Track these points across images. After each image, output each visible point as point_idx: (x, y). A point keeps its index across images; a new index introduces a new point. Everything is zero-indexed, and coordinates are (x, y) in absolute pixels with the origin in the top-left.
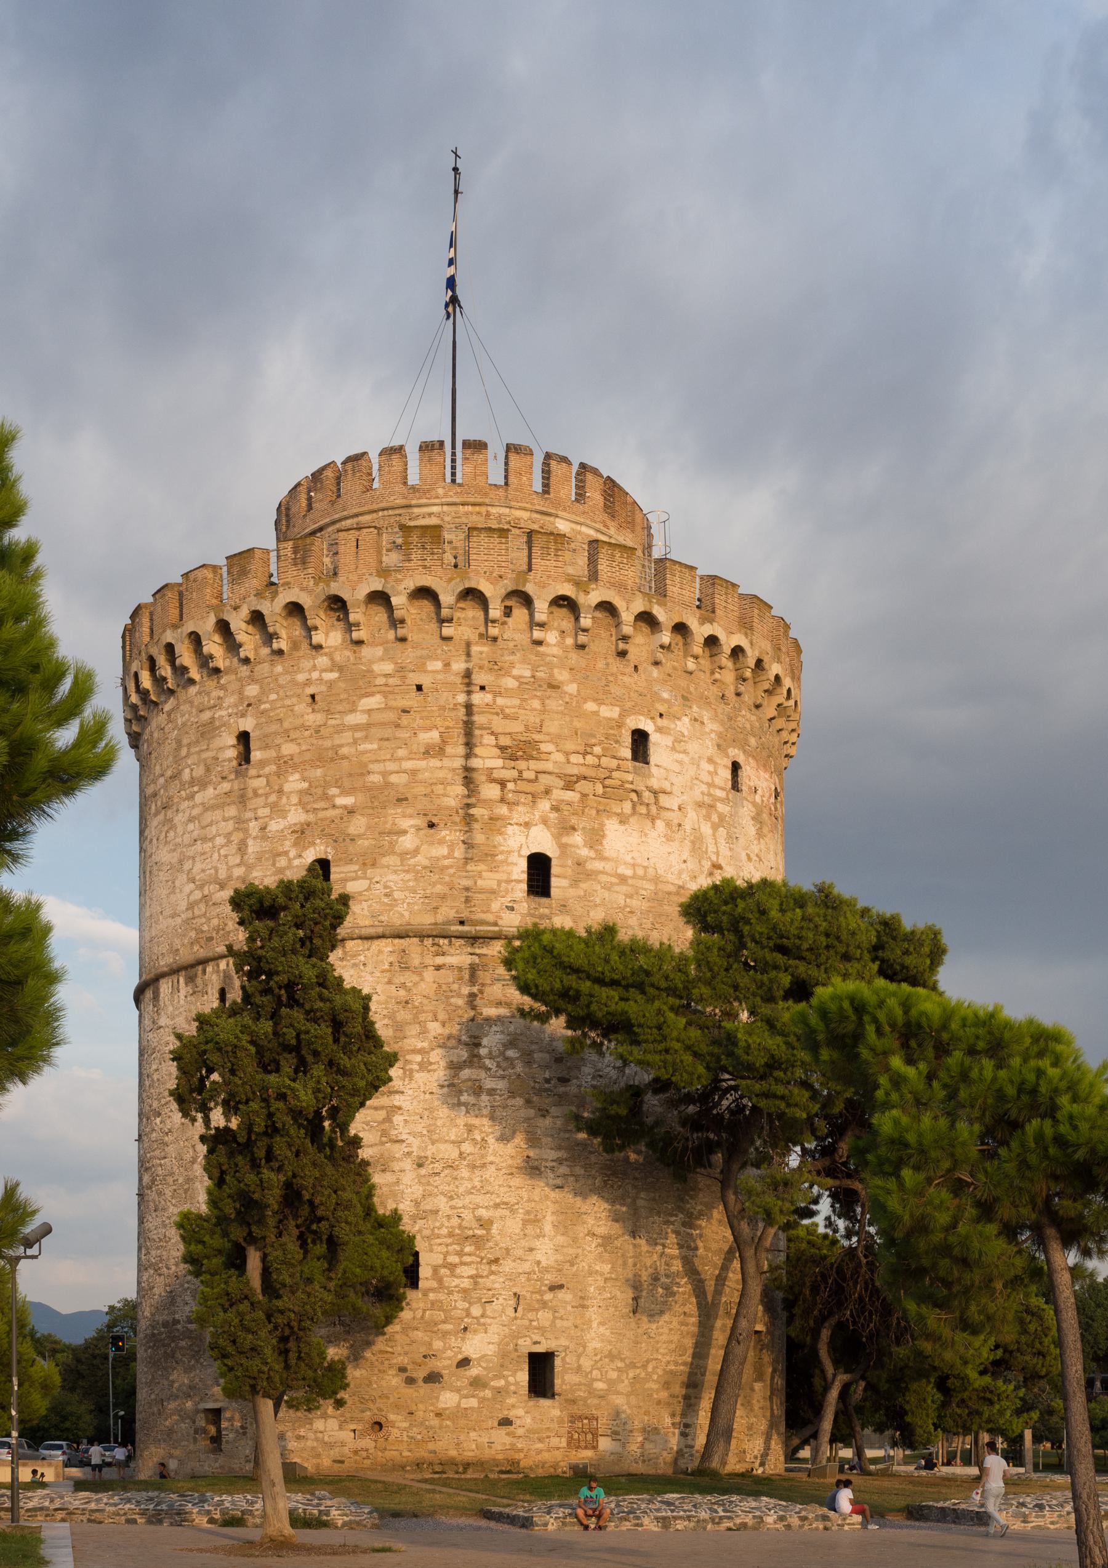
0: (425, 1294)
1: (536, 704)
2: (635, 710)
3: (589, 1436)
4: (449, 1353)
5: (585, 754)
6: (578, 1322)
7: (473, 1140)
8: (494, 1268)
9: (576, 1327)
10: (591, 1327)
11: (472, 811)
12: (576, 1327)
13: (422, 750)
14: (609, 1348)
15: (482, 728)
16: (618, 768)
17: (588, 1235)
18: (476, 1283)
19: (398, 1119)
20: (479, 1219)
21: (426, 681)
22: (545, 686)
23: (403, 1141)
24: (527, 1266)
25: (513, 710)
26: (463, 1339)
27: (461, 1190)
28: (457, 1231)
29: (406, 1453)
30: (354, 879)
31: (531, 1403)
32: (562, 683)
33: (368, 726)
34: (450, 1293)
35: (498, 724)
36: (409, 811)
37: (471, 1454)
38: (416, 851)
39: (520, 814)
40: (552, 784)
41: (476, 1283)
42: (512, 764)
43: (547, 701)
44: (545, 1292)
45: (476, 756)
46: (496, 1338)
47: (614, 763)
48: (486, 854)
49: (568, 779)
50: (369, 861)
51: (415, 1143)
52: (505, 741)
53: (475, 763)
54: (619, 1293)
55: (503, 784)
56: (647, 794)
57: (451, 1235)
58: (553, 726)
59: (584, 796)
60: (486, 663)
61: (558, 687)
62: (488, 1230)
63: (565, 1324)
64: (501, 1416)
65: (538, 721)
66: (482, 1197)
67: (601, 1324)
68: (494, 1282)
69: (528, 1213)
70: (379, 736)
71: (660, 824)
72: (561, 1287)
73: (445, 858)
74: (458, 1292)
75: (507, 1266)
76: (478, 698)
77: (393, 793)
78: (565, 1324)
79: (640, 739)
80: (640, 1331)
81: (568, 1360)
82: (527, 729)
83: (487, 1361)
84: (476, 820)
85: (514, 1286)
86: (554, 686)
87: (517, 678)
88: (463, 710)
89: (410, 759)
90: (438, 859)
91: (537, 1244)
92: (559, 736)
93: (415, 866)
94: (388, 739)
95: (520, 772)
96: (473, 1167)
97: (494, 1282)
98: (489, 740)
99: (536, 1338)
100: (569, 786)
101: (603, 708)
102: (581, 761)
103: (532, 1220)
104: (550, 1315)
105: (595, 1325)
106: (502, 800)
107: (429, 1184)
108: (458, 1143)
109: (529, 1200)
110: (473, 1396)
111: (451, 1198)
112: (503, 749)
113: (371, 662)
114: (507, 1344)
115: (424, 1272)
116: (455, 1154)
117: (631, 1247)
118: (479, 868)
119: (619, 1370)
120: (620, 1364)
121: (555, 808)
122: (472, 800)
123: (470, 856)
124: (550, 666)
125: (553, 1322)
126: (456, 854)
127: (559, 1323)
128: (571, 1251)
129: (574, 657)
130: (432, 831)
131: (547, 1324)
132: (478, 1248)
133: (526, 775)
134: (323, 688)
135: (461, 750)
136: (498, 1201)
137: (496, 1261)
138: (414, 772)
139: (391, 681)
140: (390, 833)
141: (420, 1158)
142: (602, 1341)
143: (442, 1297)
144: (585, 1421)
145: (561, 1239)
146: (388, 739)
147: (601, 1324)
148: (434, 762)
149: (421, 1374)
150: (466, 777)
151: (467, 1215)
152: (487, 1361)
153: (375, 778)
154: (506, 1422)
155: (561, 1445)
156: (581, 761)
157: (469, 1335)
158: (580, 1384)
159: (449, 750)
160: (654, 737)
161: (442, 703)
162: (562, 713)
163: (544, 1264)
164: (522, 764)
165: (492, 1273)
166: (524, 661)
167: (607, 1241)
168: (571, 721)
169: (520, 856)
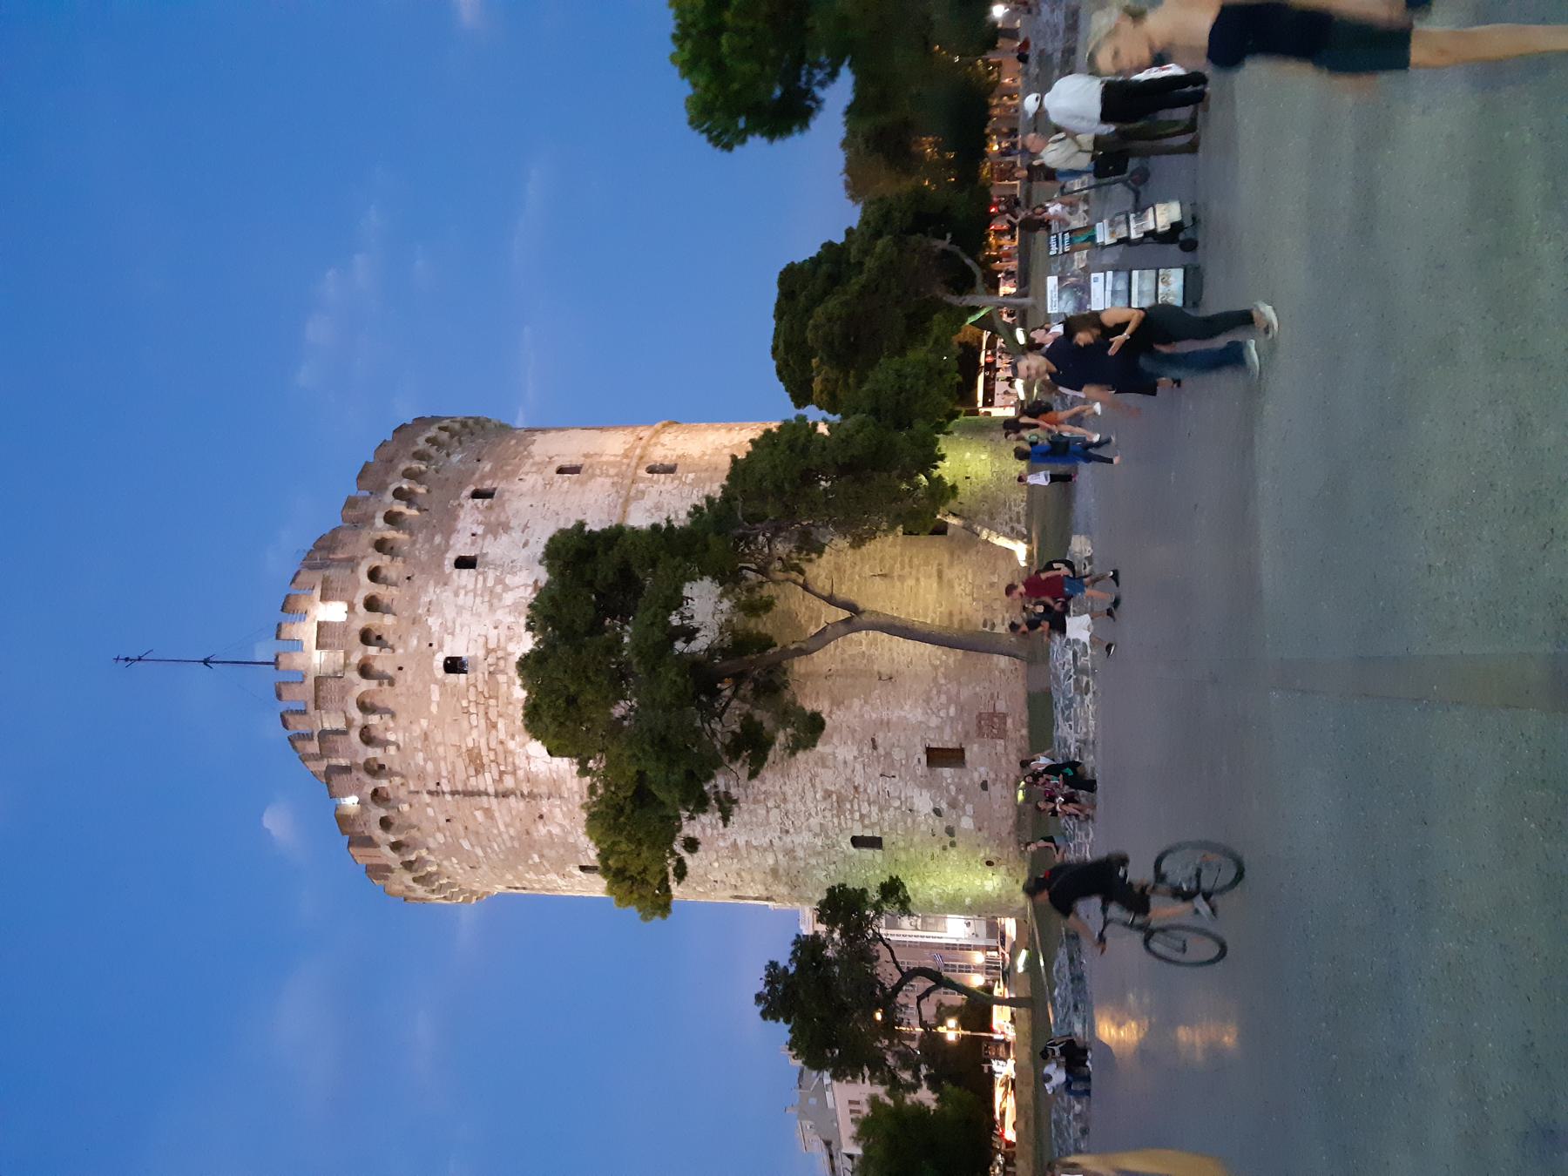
0: (885, 833)
2: (431, 671)
3: (996, 720)
4: (930, 821)
5: (468, 713)
7: (765, 799)
8: (861, 789)
9: (905, 729)
11: (526, 793)
12: (905, 729)
13: (490, 821)
14: (921, 701)
15: (466, 785)
18: (874, 802)
19: (755, 843)
20: (825, 799)
22: (427, 742)
23: (771, 841)
24: (859, 767)
25: (448, 764)
26: (918, 812)
28: (835, 812)
29: (1011, 849)
30: (589, 856)
31: (968, 766)
32: (422, 730)
37: (1011, 810)
38: (561, 825)
39: (521, 762)
41: (874, 802)
45: (486, 789)
46: (917, 791)
47: (472, 689)
53: (491, 790)
54: (877, 692)
56: (491, 660)
57: (839, 817)
58: (453, 738)
59: (500, 715)
61: (425, 734)
62: (832, 792)
63: (902, 738)
64: (980, 789)
67: (902, 708)
68: (873, 790)
69: (816, 764)
72: (873, 740)
74: (882, 813)
75: (858, 780)
76: (446, 787)
77: (524, 837)
79: (454, 665)
81: (932, 737)
82: (458, 756)
83: (935, 796)
84: (532, 790)
86: (426, 736)
88: (457, 796)
89: (498, 827)
91: (840, 758)
95: (492, 761)
96: (785, 800)
98: (473, 781)
99: (916, 761)
100: (494, 726)
103: (822, 762)
105: (903, 714)
106: (514, 773)
107: (800, 827)
109: (807, 763)
110: (964, 807)
111: (810, 814)
112: (477, 772)
113: (439, 843)
114: (921, 782)
115: (868, 833)
116: (775, 812)
119: (939, 692)
120: (934, 692)
121: (513, 737)
122: (518, 793)
127: (903, 742)
128: (845, 731)
129: (403, 720)
133: (492, 758)
134: (464, 864)
135: (485, 798)
137: (856, 788)
138: (507, 826)
139: (448, 834)
141: (781, 832)
142: (916, 707)
144: (983, 722)
145: (835, 740)
147: (902, 708)
148: (497, 814)
149: (948, 839)
150: (503, 796)
151: (821, 806)
152: (935, 796)
153: (516, 844)
154: (984, 786)
155: (1003, 744)
156: (475, 716)
157: (915, 808)
158: (951, 727)
159: (486, 806)
160: (448, 652)
163: (856, 753)
164: (485, 760)
165: (865, 790)
166: (413, 758)
169: (551, 763)
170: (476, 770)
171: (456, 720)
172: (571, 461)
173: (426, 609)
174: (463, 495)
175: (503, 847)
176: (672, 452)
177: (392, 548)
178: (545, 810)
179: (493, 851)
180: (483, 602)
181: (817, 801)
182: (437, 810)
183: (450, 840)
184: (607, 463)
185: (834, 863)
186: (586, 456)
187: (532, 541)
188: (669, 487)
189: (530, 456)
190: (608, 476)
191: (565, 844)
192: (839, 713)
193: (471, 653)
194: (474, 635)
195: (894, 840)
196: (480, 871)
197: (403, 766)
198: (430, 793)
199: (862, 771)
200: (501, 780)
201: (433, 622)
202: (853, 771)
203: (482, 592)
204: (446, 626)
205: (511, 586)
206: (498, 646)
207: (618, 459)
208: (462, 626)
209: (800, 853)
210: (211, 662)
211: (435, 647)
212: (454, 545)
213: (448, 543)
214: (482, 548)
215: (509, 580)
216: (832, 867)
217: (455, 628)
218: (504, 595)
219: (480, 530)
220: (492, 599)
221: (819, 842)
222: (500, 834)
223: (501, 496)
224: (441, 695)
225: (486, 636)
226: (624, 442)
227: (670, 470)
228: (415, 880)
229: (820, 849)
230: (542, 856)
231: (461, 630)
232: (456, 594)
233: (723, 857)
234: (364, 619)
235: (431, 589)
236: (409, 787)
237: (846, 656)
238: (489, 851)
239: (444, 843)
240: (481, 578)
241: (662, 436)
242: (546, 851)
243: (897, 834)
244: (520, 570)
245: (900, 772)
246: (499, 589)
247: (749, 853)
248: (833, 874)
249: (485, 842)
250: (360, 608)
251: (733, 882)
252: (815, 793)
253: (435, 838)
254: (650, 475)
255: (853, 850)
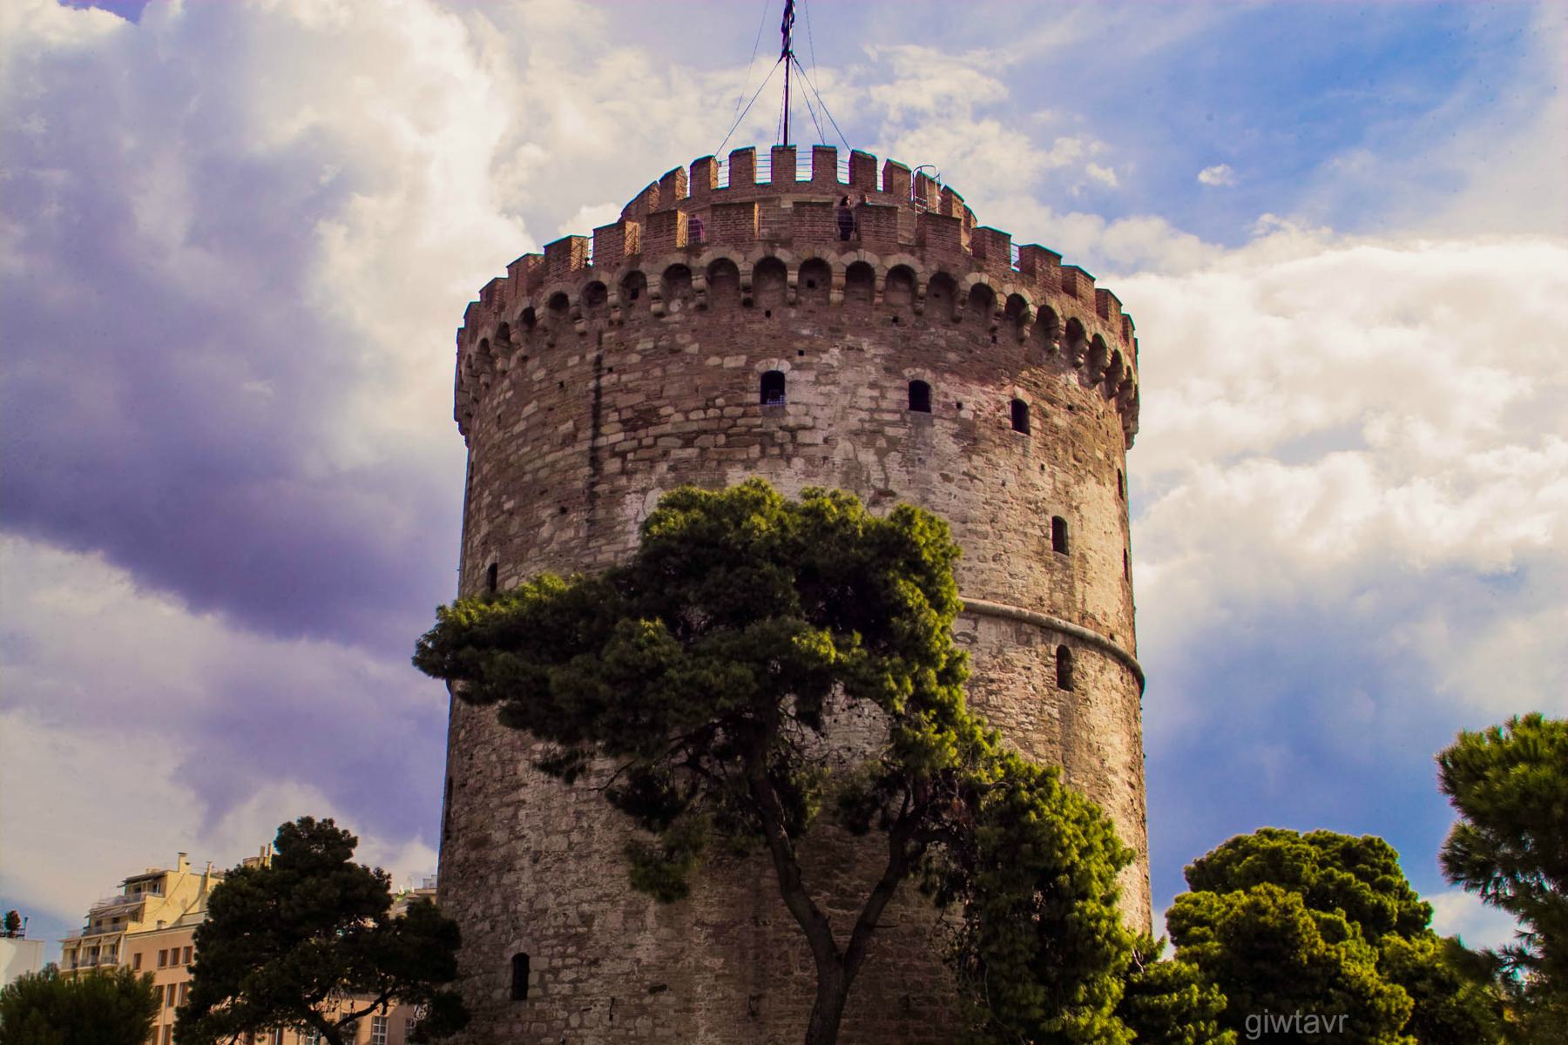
0: (532, 1005)
1: (657, 372)
5: (705, 409)
6: (682, 1029)
7: (582, 827)
8: (593, 970)
10: (697, 1035)
11: (598, 489)
12: (679, 1035)
13: (560, 441)
15: (609, 407)
16: (744, 415)
17: (695, 925)
18: (576, 988)
19: (522, 813)
20: (582, 915)
21: (564, 376)
23: (524, 837)
24: (626, 966)
27: (568, 884)
28: (562, 931)
32: (684, 346)
33: (527, 430)
34: (552, 1002)
35: (623, 400)
36: (547, 502)
39: (639, 481)
40: (669, 444)
41: (576, 988)
42: (633, 434)
43: (668, 367)
44: (645, 995)
45: (602, 435)
47: (740, 410)
48: (606, 528)
49: (687, 436)
50: (519, 558)
51: (532, 836)
52: (627, 414)
53: (602, 441)
54: (733, 993)
55: (623, 455)
57: (556, 935)
58: (671, 390)
59: (703, 450)
60: (614, 346)
63: (666, 1032)
65: (658, 387)
66: (586, 890)
67: (710, 1030)
69: (630, 904)
70: (533, 438)
71: (798, 463)
73: (572, 539)
74: (559, 1000)
75: (607, 967)
76: (606, 381)
78: (666, 1032)
79: (773, 385)
80: (763, 1038)
82: (648, 397)
84: (599, 497)
85: (612, 989)
86: (675, 351)
87: (639, 353)
88: (593, 395)
89: (551, 452)
90: (566, 542)
92: (679, 397)
93: (549, 553)
94: (537, 439)
96: (579, 857)
97: (593, 986)
98: (614, 416)
100: (688, 441)
101: (727, 360)
102: (702, 415)
103: (634, 913)
104: (649, 1023)
105: (702, 1032)
106: (624, 472)
107: (541, 880)
108: (567, 833)
111: (559, 894)
112: (623, 422)
113: (532, 373)
115: (533, 979)
116: (565, 846)
117: (752, 936)
118: (599, 543)
121: (672, 469)
123: (591, 533)
124: (673, 333)
125: (653, 1030)
126: (581, 534)
127: (659, 1031)
128: (676, 945)
129: (696, 320)
130: (564, 516)
131: (645, 1032)
132: (580, 948)
133: (645, 442)
135: (589, 433)
136: (600, 892)
138: (554, 463)
139: (544, 385)
140: (532, 528)
141: (536, 852)
143: (546, 1006)
145: (664, 932)
146: (537, 439)
147: (710, 1030)
148: (569, 450)
150: (592, 459)
151: (572, 912)
153: (528, 478)
159: (581, 435)
160: (791, 376)
161: (577, 393)
162: (682, 374)
163: (644, 962)
164: (642, 433)
165: (592, 976)
166: (648, 335)
167: (719, 931)
168: (692, 380)
170: (629, 420)
171: (697, 391)
172: (1072, 538)
173: (850, 344)
174: (1016, 388)
175: (526, 459)
176: (1091, 685)
177: (937, 296)
178: (573, 517)
179: (519, 448)
180: (861, 421)
181: (578, 905)
182: (576, 370)
183: (536, 387)
184: (1072, 587)
185: (493, 928)
186: (1083, 557)
187: (953, 488)
188: (1038, 682)
189: (1080, 480)
190: (1052, 591)
191: (528, 544)
192: (702, 937)
193: (790, 409)
194: (817, 412)
195: (523, 1017)
196: (494, 429)
197: (636, 323)
198: (599, 360)
199: (619, 972)
200: (614, 454)
201: (833, 356)
202: (620, 958)
203: (877, 421)
204: (827, 374)
205: (886, 460)
206: (800, 445)
207: (1079, 605)
208: (828, 395)
209: (508, 879)
210: (788, 61)
211: (798, 359)
212: (944, 380)
213: (946, 372)
214: (940, 417)
215: (894, 459)
216: (487, 926)
217: (825, 385)
218: (872, 451)
219: (966, 414)
220: (868, 435)
221: (522, 907)
222: (542, 456)
223: (1016, 440)
224: (735, 369)
225: (813, 428)
226: (1105, 614)
227: (1064, 679)
228: (485, 342)
229: (512, 907)
230: (511, 513)
231: (821, 394)
232: (873, 386)
233: (503, 769)
234: (838, 260)
235: (881, 351)
236: (607, 331)
237: (785, 947)
238: (520, 441)
239: (531, 381)
240: (897, 417)
241: (1117, 667)
242: (517, 520)
243: (531, 1023)
244: (908, 472)
245: (619, 1028)
246: (882, 443)
247: (508, 805)
248: (478, 927)
249: (531, 435)
250: (850, 258)
251: (471, 781)
252: (589, 902)
253: (538, 368)
254: (1054, 652)
255: (510, 956)
